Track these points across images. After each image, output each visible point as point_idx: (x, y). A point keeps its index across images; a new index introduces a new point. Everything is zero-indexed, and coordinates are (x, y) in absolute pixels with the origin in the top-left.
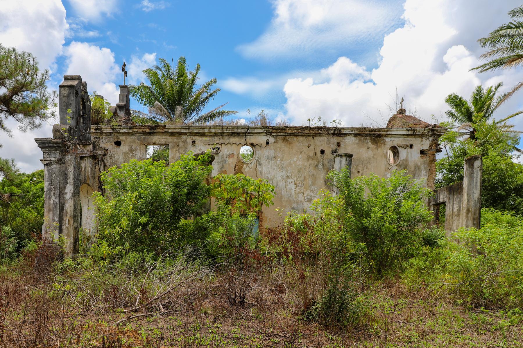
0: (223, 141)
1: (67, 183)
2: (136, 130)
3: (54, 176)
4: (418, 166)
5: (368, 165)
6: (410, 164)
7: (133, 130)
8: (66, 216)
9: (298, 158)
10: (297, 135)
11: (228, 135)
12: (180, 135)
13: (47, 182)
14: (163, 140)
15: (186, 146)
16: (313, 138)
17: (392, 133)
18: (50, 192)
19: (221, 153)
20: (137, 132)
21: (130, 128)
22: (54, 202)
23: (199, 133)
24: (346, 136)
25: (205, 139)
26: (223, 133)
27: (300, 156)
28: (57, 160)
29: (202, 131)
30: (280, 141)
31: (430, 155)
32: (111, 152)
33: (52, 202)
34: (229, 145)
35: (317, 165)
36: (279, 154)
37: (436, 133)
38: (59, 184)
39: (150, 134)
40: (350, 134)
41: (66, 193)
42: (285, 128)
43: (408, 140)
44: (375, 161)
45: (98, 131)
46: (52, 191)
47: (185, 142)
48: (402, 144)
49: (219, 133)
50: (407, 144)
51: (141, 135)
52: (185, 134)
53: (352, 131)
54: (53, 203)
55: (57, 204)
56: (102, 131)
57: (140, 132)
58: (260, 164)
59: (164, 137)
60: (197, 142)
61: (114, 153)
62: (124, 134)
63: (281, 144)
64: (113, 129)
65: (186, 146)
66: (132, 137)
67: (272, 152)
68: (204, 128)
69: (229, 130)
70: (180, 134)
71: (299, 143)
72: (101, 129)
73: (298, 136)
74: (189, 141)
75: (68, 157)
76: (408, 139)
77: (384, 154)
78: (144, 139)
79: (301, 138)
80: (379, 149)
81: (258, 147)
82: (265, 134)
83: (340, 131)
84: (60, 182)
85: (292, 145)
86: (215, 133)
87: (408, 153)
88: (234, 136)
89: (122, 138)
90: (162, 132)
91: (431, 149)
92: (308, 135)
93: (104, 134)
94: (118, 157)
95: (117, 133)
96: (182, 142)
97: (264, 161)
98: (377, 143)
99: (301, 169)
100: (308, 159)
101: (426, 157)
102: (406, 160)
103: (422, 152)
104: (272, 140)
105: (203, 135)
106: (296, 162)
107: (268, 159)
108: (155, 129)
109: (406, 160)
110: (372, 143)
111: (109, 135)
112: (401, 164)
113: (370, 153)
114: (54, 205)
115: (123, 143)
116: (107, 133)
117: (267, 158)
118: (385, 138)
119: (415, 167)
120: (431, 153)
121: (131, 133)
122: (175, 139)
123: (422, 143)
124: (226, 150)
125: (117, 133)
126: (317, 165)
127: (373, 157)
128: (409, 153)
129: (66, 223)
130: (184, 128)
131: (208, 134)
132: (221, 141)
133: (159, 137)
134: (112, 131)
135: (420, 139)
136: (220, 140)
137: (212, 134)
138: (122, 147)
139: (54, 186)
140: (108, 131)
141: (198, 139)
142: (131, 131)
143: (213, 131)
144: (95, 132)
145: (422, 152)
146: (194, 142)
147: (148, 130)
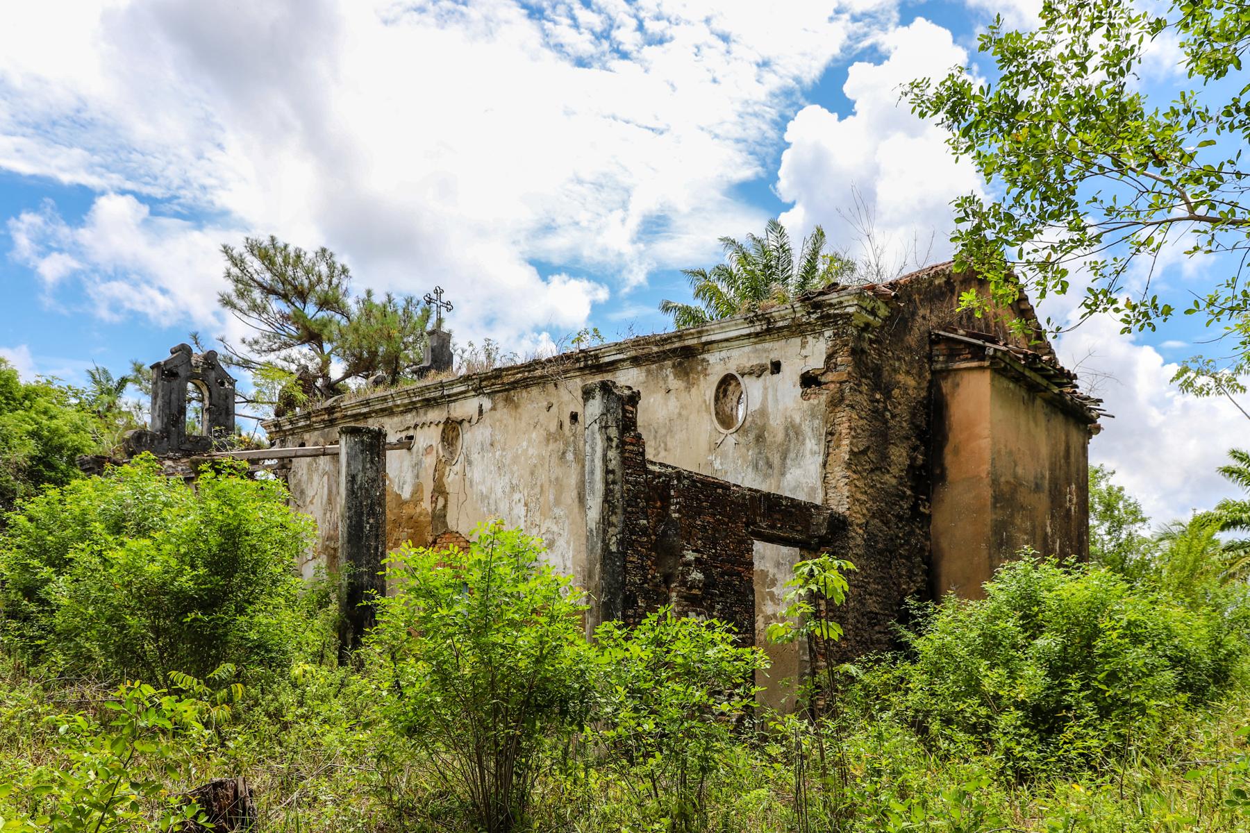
2: (314, 419)
4: (793, 426)
5: (668, 438)
6: (771, 422)
9: (530, 441)
10: (525, 384)
16: (556, 385)
17: (714, 338)
24: (617, 369)
26: (414, 403)
27: (534, 435)
30: (501, 405)
35: (564, 453)
36: (499, 437)
37: (832, 311)
40: (623, 360)
42: (498, 373)
43: (765, 351)
44: (685, 426)
53: (620, 351)
58: (470, 463)
63: (503, 413)
66: (316, 433)
67: (488, 432)
71: (532, 401)
73: (527, 386)
76: (767, 345)
77: (705, 401)
79: (535, 391)
80: (694, 390)
81: (466, 424)
82: (473, 393)
83: (596, 357)
85: (519, 410)
87: (766, 389)
88: (433, 407)
91: (836, 364)
92: (542, 381)
97: (476, 456)
98: (687, 374)
99: (535, 466)
100: (548, 440)
102: (763, 412)
103: (809, 381)
104: (487, 403)
106: (527, 450)
107: (482, 449)
109: (763, 412)
110: (676, 376)
113: (673, 404)
117: (479, 447)
118: (706, 356)
119: (787, 429)
120: (834, 379)
123: (804, 352)
126: (564, 453)
127: (680, 414)
128: (770, 390)
135: (798, 341)
145: (809, 381)
147: (326, 417)
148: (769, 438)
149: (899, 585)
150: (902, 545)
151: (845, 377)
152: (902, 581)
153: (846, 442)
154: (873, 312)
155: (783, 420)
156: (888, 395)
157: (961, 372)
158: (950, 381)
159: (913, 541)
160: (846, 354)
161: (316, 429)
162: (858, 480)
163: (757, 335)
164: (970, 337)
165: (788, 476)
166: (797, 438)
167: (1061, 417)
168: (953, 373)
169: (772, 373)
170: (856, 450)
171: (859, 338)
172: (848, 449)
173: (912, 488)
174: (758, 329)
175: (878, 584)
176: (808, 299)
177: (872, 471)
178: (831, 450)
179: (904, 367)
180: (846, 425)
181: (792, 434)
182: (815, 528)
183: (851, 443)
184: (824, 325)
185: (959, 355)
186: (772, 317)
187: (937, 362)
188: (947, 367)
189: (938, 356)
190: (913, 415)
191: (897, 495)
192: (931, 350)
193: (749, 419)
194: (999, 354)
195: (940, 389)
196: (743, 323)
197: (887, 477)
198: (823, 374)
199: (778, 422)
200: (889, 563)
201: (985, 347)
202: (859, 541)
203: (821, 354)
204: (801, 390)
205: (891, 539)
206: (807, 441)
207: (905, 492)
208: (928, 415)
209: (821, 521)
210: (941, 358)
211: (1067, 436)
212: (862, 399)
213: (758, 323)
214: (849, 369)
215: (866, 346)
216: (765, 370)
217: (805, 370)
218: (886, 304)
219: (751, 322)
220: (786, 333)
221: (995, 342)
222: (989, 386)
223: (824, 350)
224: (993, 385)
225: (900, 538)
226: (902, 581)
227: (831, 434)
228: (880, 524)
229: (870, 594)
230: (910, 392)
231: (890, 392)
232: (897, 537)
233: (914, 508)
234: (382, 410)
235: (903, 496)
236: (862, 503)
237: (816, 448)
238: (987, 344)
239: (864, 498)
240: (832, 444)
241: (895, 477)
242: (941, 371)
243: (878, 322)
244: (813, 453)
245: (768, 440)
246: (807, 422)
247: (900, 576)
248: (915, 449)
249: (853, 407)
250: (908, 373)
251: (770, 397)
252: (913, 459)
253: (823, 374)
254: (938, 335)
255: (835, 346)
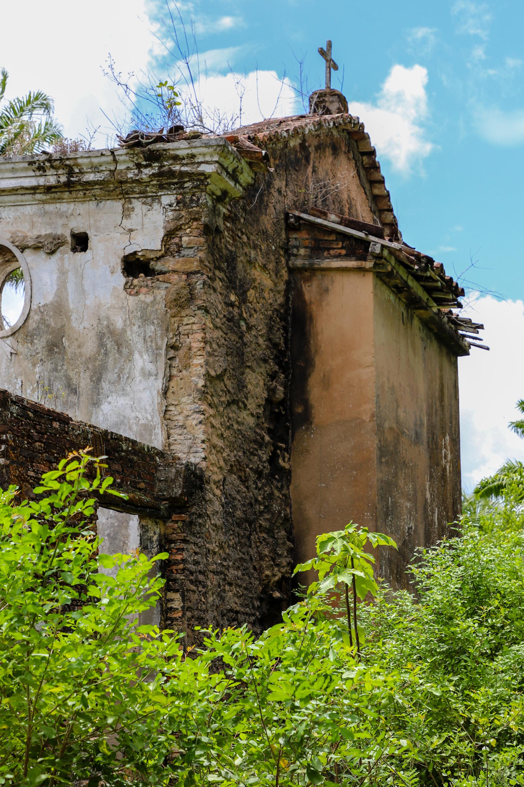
4: (112, 333)
6: (74, 324)
31: (175, 278)
43: (61, 215)
48: (36, 233)
50: (59, 232)
76: (63, 207)
87: (63, 273)
91: (179, 247)
101: (151, 289)
112: (32, 324)
119: (101, 337)
120: (177, 267)
123: (128, 224)
128: (71, 277)
135: (117, 205)
148: (71, 348)
149: (260, 570)
150: (261, 513)
151: (195, 266)
152: (264, 564)
153: (199, 361)
154: (234, 176)
155: (95, 323)
156: (243, 299)
157: (332, 274)
158: (315, 284)
159: (275, 507)
160: (196, 232)
162: (214, 416)
163: (49, 189)
164: (346, 226)
165: (105, 407)
166: (119, 352)
167: (435, 345)
168: (319, 274)
169: (74, 250)
170: (213, 373)
171: (214, 211)
172: (203, 371)
173: (270, 432)
174: (52, 180)
175: (238, 568)
176: (139, 144)
177: (229, 404)
178: (174, 372)
179: (261, 260)
180: (199, 336)
181: (110, 344)
182: (162, 485)
183: (207, 363)
184: (161, 187)
185: (329, 249)
186: (77, 165)
187: (296, 256)
188: (311, 264)
189: (297, 248)
190: (270, 328)
191: (255, 441)
192: (288, 239)
193: (36, 317)
194: (386, 253)
195: (300, 294)
196: (25, 169)
197: (244, 414)
198: (158, 259)
199: (86, 324)
200: (249, 538)
201: (369, 243)
202: (217, 506)
203: (156, 228)
204: (122, 280)
205: (251, 504)
206: (136, 356)
207: (263, 438)
208: (285, 329)
209: (172, 475)
210: (302, 251)
211: (441, 370)
212: (216, 299)
213: (52, 171)
214: (201, 254)
215: (220, 222)
216: (62, 244)
217: (129, 251)
218: (250, 164)
219: (40, 168)
220: (97, 192)
221: (381, 237)
222: (372, 296)
223: (161, 224)
224: (375, 295)
225: (260, 504)
226: (264, 564)
227: (174, 347)
228: (237, 482)
229: (230, 584)
230: (266, 295)
231: (245, 292)
232: (256, 500)
233: (273, 460)
235: (261, 444)
236: (220, 451)
237: (150, 367)
238: (372, 238)
239: (220, 443)
240: (176, 363)
241: (252, 415)
242: (302, 270)
243: (237, 191)
244: (146, 375)
245: (69, 351)
246: (135, 328)
247: (262, 558)
248: (273, 376)
249: (207, 311)
250: (264, 268)
251: (71, 287)
252: (272, 391)
253: (158, 259)
254: (298, 218)
255: (178, 218)
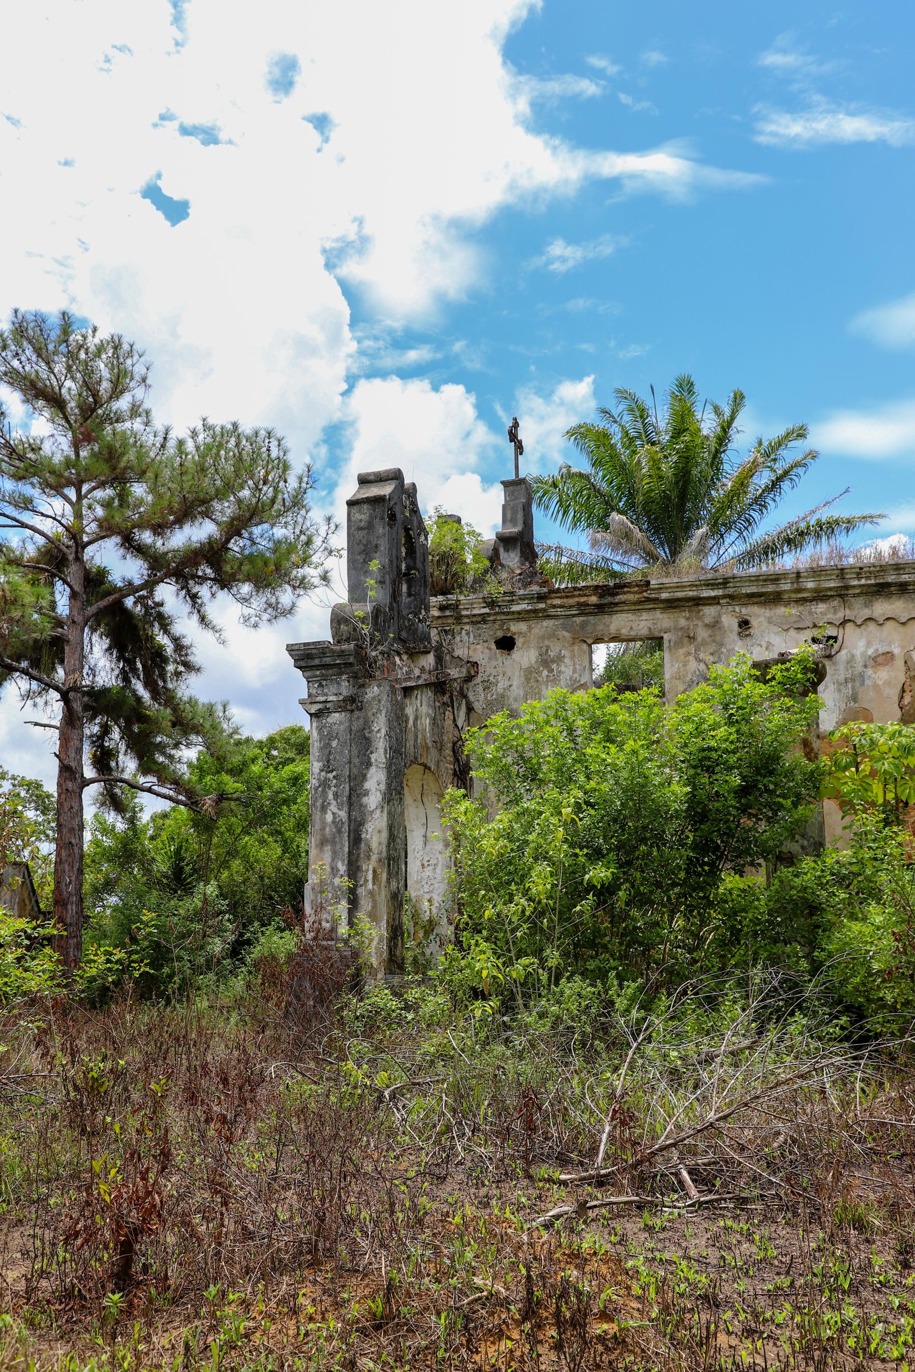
0: (849, 614)
1: (369, 764)
2: (557, 602)
3: (334, 744)
7: (549, 602)
8: (369, 858)
11: (866, 594)
12: (698, 605)
13: (318, 761)
14: (643, 624)
15: (718, 638)
18: (324, 791)
19: (843, 652)
20: (561, 607)
21: (541, 598)
22: (335, 818)
23: (760, 595)
25: (782, 610)
26: (847, 587)
28: (344, 701)
29: (771, 588)
32: (488, 669)
33: (329, 817)
34: (872, 626)
38: (347, 766)
39: (601, 609)
41: (367, 793)
45: (448, 613)
46: (330, 787)
47: (715, 625)
49: (830, 589)
51: (574, 616)
52: (714, 601)
54: (333, 822)
55: (343, 823)
56: (459, 613)
57: (571, 607)
59: (645, 616)
60: (754, 623)
61: (494, 672)
62: (521, 616)
64: (492, 604)
65: (718, 638)
66: (546, 623)
68: (777, 579)
69: (868, 578)
70: (698, 602)
72: (455, 607)
74: (730, 621)
75: (373, 691)
78: (583, 626)
84: (350, 762)
86: (816, 590)
88: (889, 595)
89: (516, 627)
90: (640, 602)
93: (466, 620)
94: (507, 683)
95: (504, 613)
96: (706, 625)
105: (776, 599)
108: (617, 594)
111: (479, 622)
114: (336, 827)
115: (519, 642)
116: (474, 615)
121: (544, 610)
122: (682, 619)
124: (862, 644)
125: (504, 613)
129: (366, 881)
130: (710, 584)
131: (793, 596)
132: (840, 615)
133: (630, 616)
134: (487, 610)
136: (835, 612)
137: (805, 595)
138: (516, 654)
139: (334, 773)
140: (476, 612)
141: (758, 615)
142: (542, 606)
143: (810, 585)
144: (439, 617)
146: (744, 624)
147: (594, 599)
161: (549, 617)
234: (751, 596)
